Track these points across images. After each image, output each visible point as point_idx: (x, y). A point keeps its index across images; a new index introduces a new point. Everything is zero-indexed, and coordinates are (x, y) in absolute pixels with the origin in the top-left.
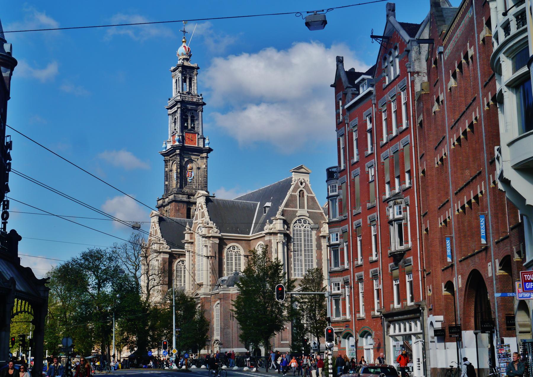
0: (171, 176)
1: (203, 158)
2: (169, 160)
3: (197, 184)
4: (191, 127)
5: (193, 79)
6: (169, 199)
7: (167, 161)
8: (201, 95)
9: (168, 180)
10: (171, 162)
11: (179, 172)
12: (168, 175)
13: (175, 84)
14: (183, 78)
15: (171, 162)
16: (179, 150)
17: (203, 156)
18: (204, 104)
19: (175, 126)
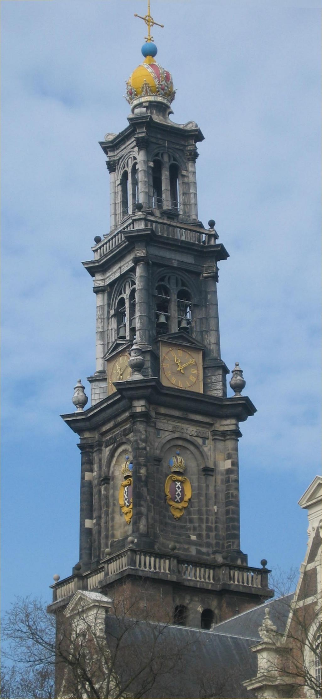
0: (107, 497)
1: (224, 434)
2: (100, 444)
3: (204, 526)
4: (181, 329)
5: (184, 173)
6: (107, 574)
7: (91, 446)
8: (212, 224)
9: (95, 514)
10: (107, 451)
11: (143, 478)
12: (96, 497)
13: (120, 188)
14: (151, 164)
15: (107, 451)
16: (142, 403)
17: (222, 429)
18: (222, 254)
19: (118, 329)
